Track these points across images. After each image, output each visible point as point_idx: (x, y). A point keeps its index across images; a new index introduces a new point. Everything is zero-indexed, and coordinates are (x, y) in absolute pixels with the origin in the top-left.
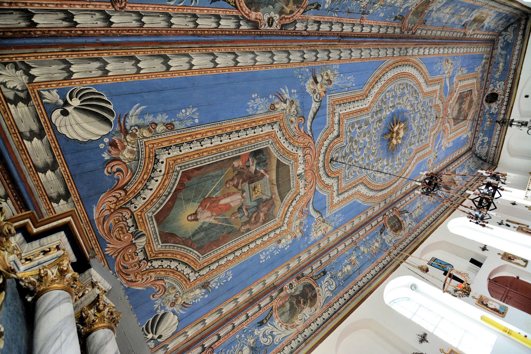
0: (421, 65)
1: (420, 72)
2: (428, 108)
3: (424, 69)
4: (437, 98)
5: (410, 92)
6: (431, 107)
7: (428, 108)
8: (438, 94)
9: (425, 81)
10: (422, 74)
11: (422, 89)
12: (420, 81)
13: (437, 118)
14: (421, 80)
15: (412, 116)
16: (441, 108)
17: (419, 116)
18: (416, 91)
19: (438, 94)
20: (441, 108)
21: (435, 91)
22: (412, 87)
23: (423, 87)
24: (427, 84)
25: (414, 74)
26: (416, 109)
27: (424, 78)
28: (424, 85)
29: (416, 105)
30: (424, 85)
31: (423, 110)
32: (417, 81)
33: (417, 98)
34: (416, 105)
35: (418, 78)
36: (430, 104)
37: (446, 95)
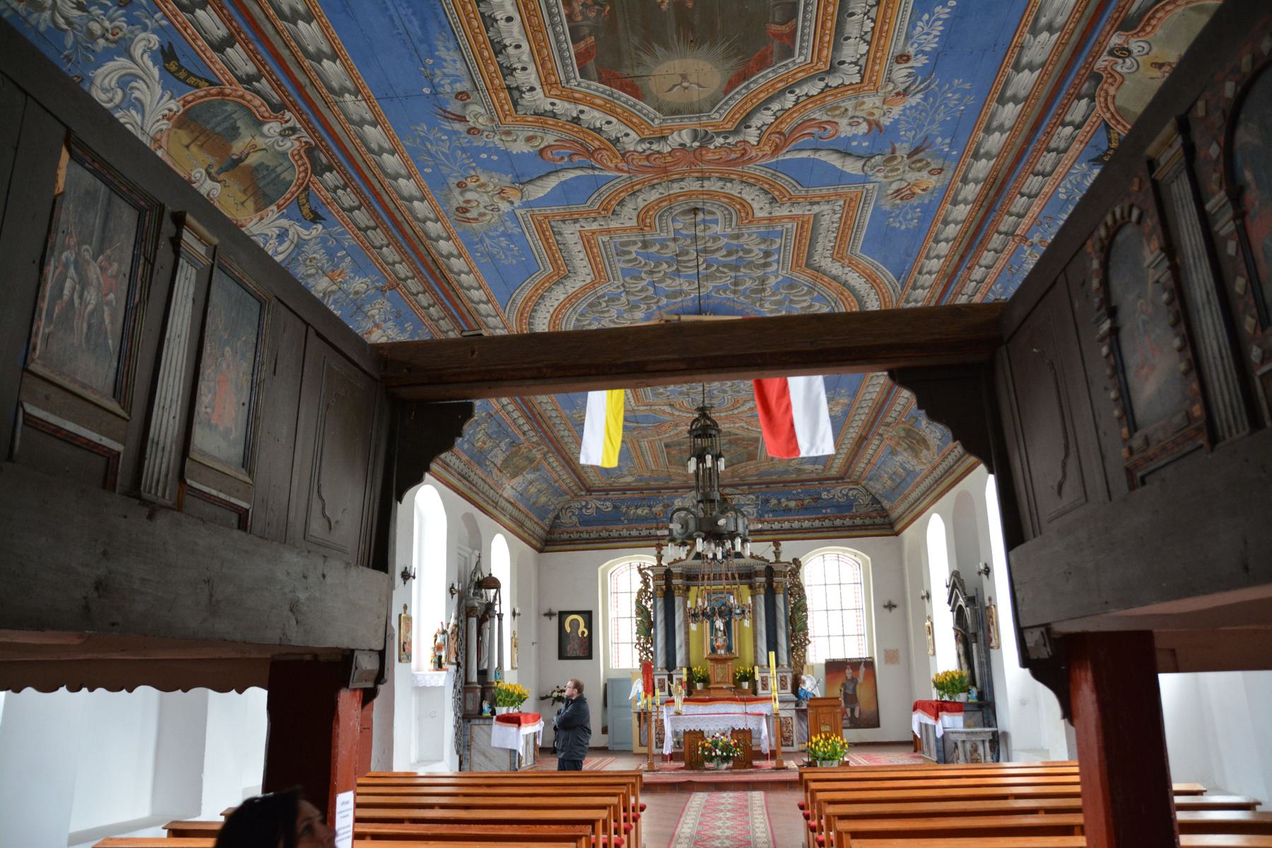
0: (519, 302)
1: (538, 304)
2: (648, 257)
3: (526, 293)
4: (613, 225)
5: (596, 319)
6: (645, 245)
7: (648, 257)
8: (595, 226)
9: (557, 283)
10: (542, 297)
11: (584, 289)
12: (562, 297)
13: (695, 211)
14: (559, 295)
15: (664, 301)
16: (654, 196)
17: (669, 281)
18: (591, 305)
19: (595, 226)
20: (654, 196)
21: (587, 241)
22: (582, 315)
23: (579, 285)
24: (566, 277)
25: (548, 316)
26: (644, 295)
27: (550, 290)
28: (573, 286)
29: (632, 298)
30: (573, 286)
31: (651, 273)
32: (562, 306)
33: (613, 299)
34: (632, 298)
35: (556, 304)
36: (633, 249)
37: (597, 183)
